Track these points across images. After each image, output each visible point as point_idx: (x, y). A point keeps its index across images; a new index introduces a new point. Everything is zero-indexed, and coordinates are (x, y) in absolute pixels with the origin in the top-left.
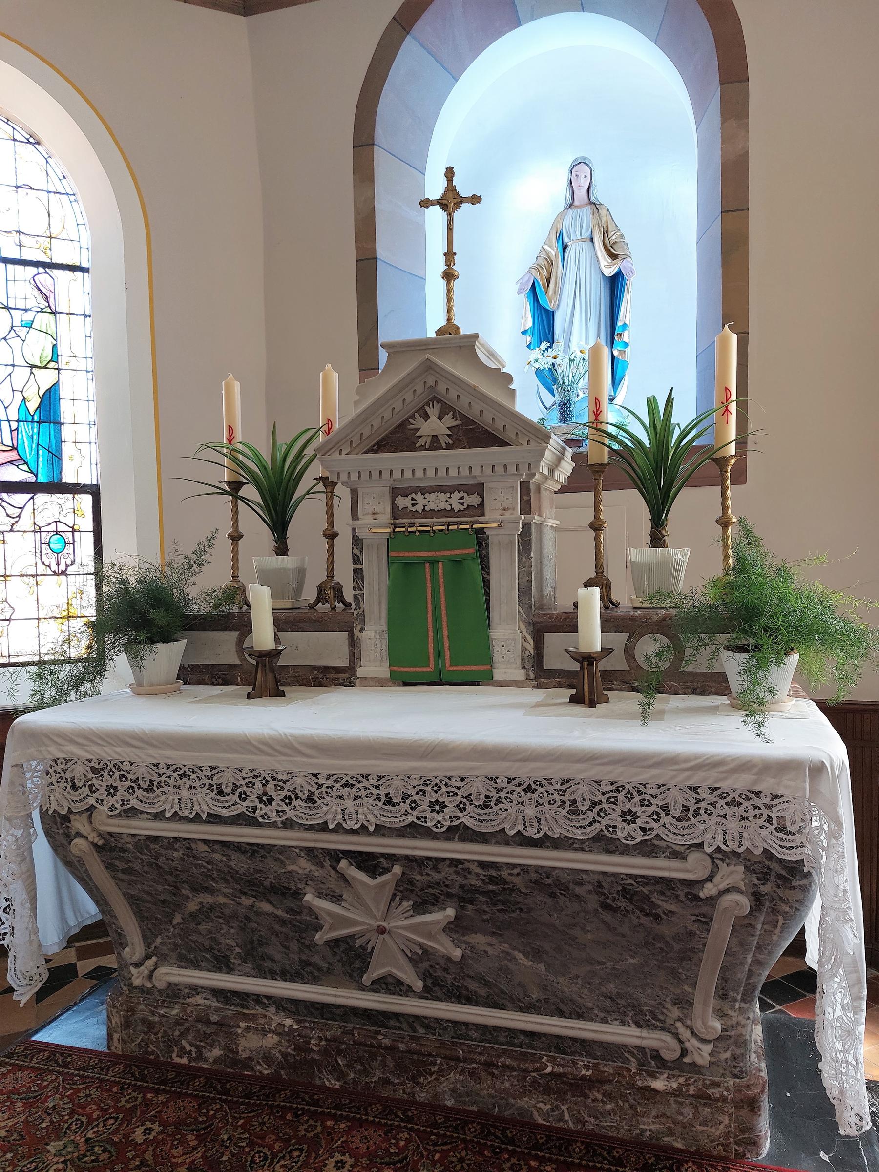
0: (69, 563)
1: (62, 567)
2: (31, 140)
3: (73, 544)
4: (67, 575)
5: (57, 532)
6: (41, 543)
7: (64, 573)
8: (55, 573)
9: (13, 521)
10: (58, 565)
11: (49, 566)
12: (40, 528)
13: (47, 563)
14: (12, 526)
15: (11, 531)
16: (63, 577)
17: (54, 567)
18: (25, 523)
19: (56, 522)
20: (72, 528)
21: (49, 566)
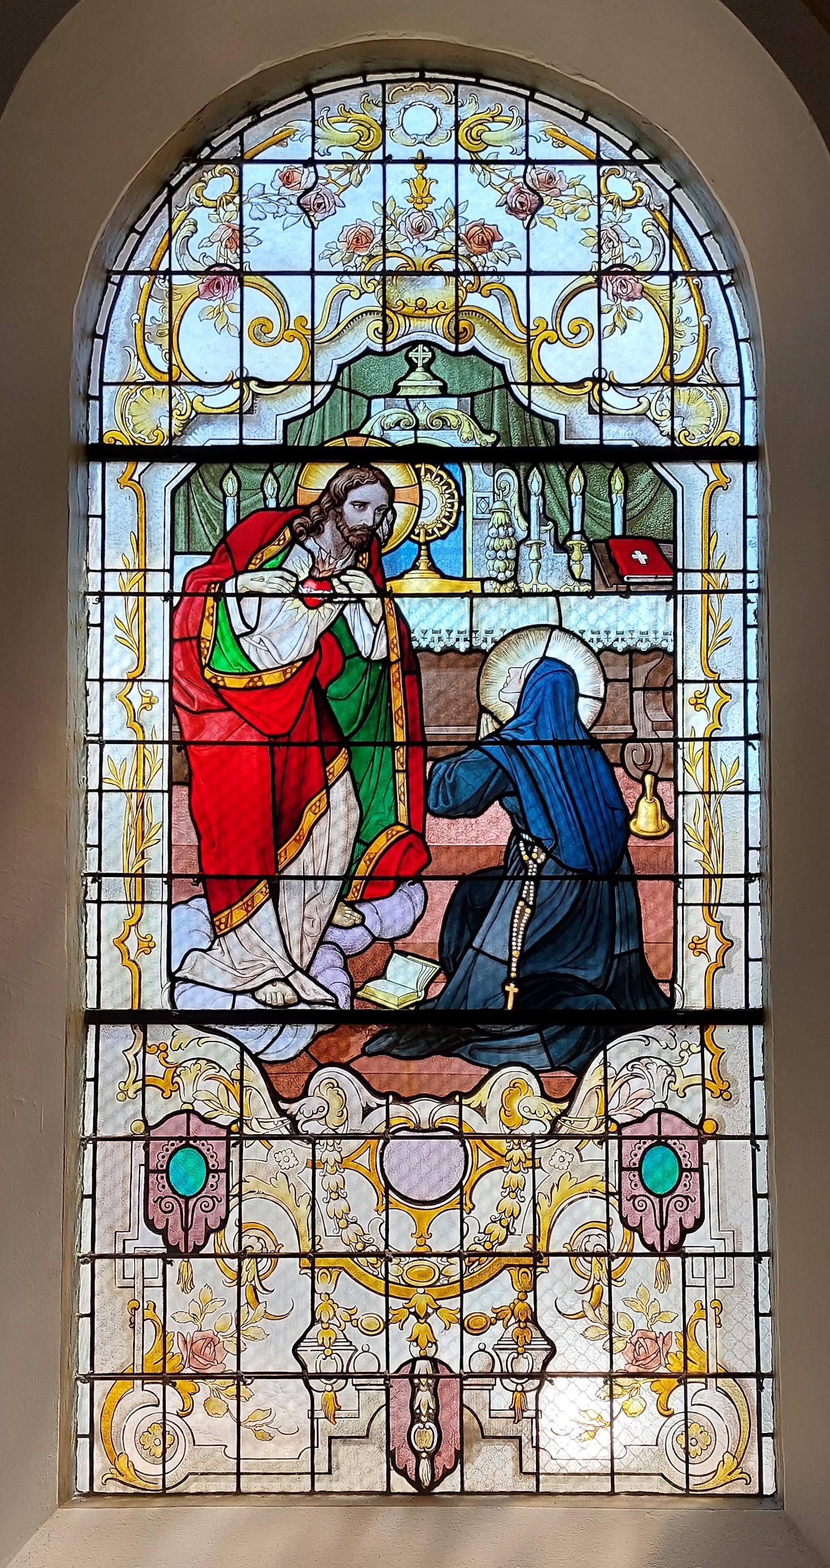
0: (689, 1223)
1: (671, 1236)
2: (638, 154)
3: (700, 1170)
4: (684, 1256)
5: (661, 1140)
6: (621, 1169)
7: (677, 1250)
8: (652, 1251)
9: (555, 1108)
10: (662, 1229)
11: (638, 1229)
12: (621, 1126)
13: (633, 1222)
14: (554, 1123)
15: (553, 1134)
16: (675, 1262)
17: (653, 1237)
18: (585, 1111)
19: (659, 1111)
20: (700, 1127)
21: (638, 1229)
